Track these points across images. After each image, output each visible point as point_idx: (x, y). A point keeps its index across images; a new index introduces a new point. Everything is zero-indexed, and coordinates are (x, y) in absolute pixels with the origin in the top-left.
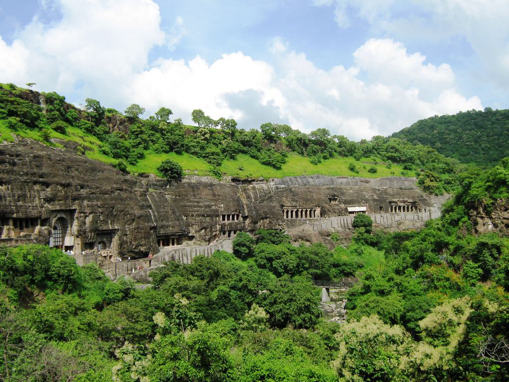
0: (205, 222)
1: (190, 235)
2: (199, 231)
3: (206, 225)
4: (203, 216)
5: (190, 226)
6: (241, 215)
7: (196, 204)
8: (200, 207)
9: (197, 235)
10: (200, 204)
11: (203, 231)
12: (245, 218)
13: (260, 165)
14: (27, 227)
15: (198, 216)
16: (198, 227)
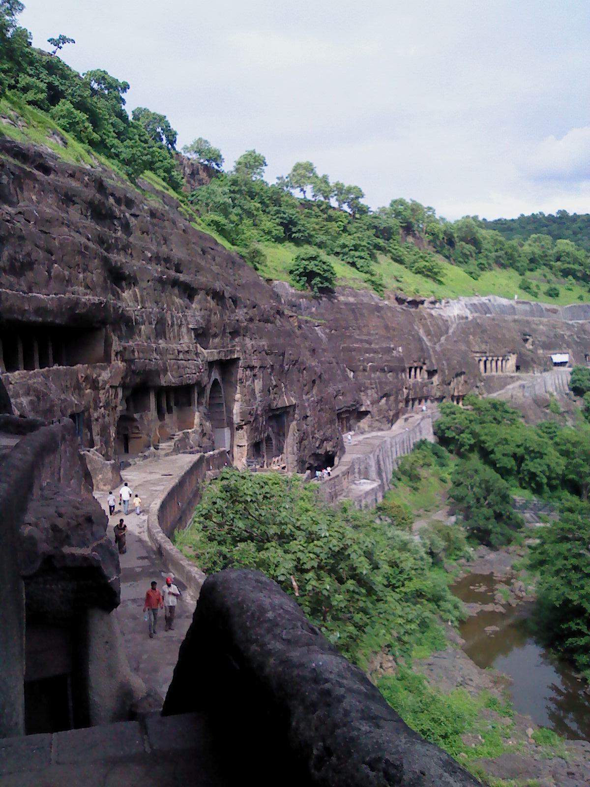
0: (386, 383)
1: (363, 409)
2: (379, 401)
3: (388, 388)
4: (383, 370)
5: (361, 391)
6: (425, 367)
7: (367, 346)
8: (375, 352)
9: (374, 410)
10: (373, 346)
11: (384, 400)
12: (431, 373)
13: (414, 275)
14: (170, 411)
15: (374, 369)
16: (377, 393)
